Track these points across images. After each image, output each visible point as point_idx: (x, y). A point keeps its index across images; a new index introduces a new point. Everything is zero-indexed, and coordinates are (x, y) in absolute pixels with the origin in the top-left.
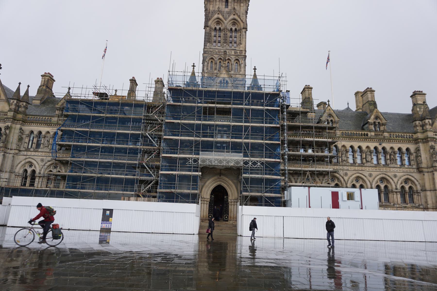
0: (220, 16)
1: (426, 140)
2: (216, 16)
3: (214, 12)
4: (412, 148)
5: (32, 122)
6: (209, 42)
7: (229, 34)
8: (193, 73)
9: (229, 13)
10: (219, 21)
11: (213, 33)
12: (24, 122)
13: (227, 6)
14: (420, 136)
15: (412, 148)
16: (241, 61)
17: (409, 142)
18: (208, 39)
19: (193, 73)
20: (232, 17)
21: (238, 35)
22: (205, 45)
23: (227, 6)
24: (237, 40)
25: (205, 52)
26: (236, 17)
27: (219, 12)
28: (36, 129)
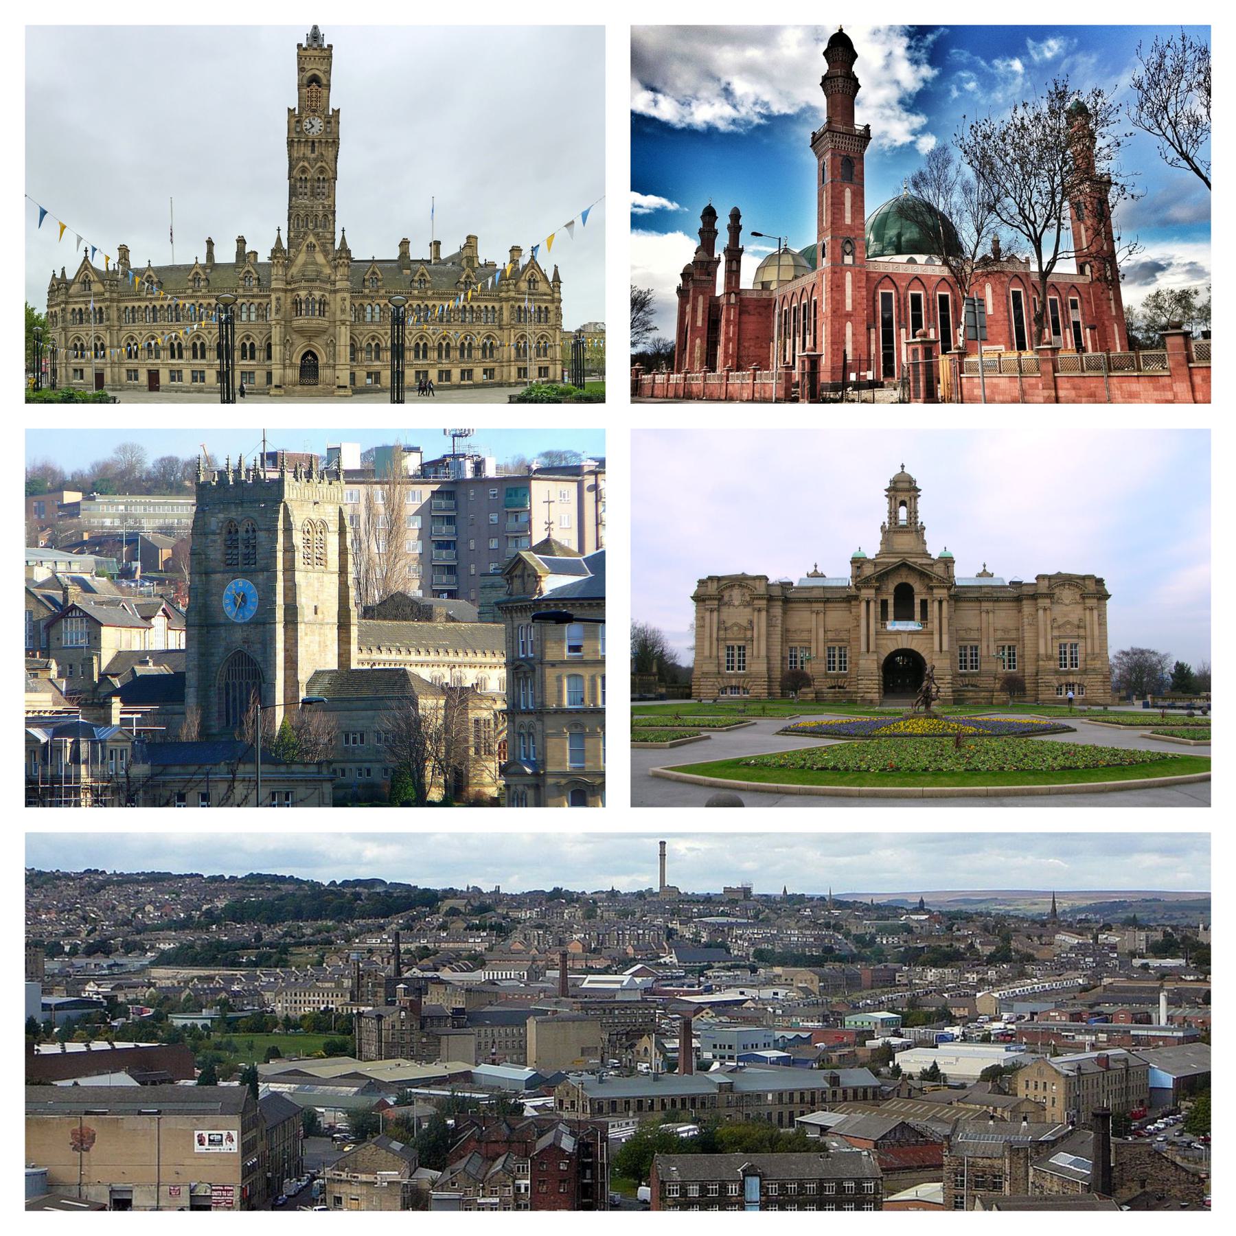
0: (306, 164)
1: (507, 300)
2: (301, 164)
3: (299, 159)
4: (497, 306)
5: (123, 301)
6: (296, 196)
7: (316, 184)
8: (279, 239)
9: (316, 160)
10: (304, 170)
11: (298, 184)
12: (119, 301)
13: (313, 151)
14: (502, 294)
15: (497, 306)
16: (331, 217)
17: (495, 300)
18: (293, 193)
19: (279, 239)
20: (319, 164)
21: (326, 185)
22: (290, 200)
23: (313, 151)
24: (326, 191)
25: (290, 208)
26: (324, 164)
27: (305, 158)
28: (130, 305)
